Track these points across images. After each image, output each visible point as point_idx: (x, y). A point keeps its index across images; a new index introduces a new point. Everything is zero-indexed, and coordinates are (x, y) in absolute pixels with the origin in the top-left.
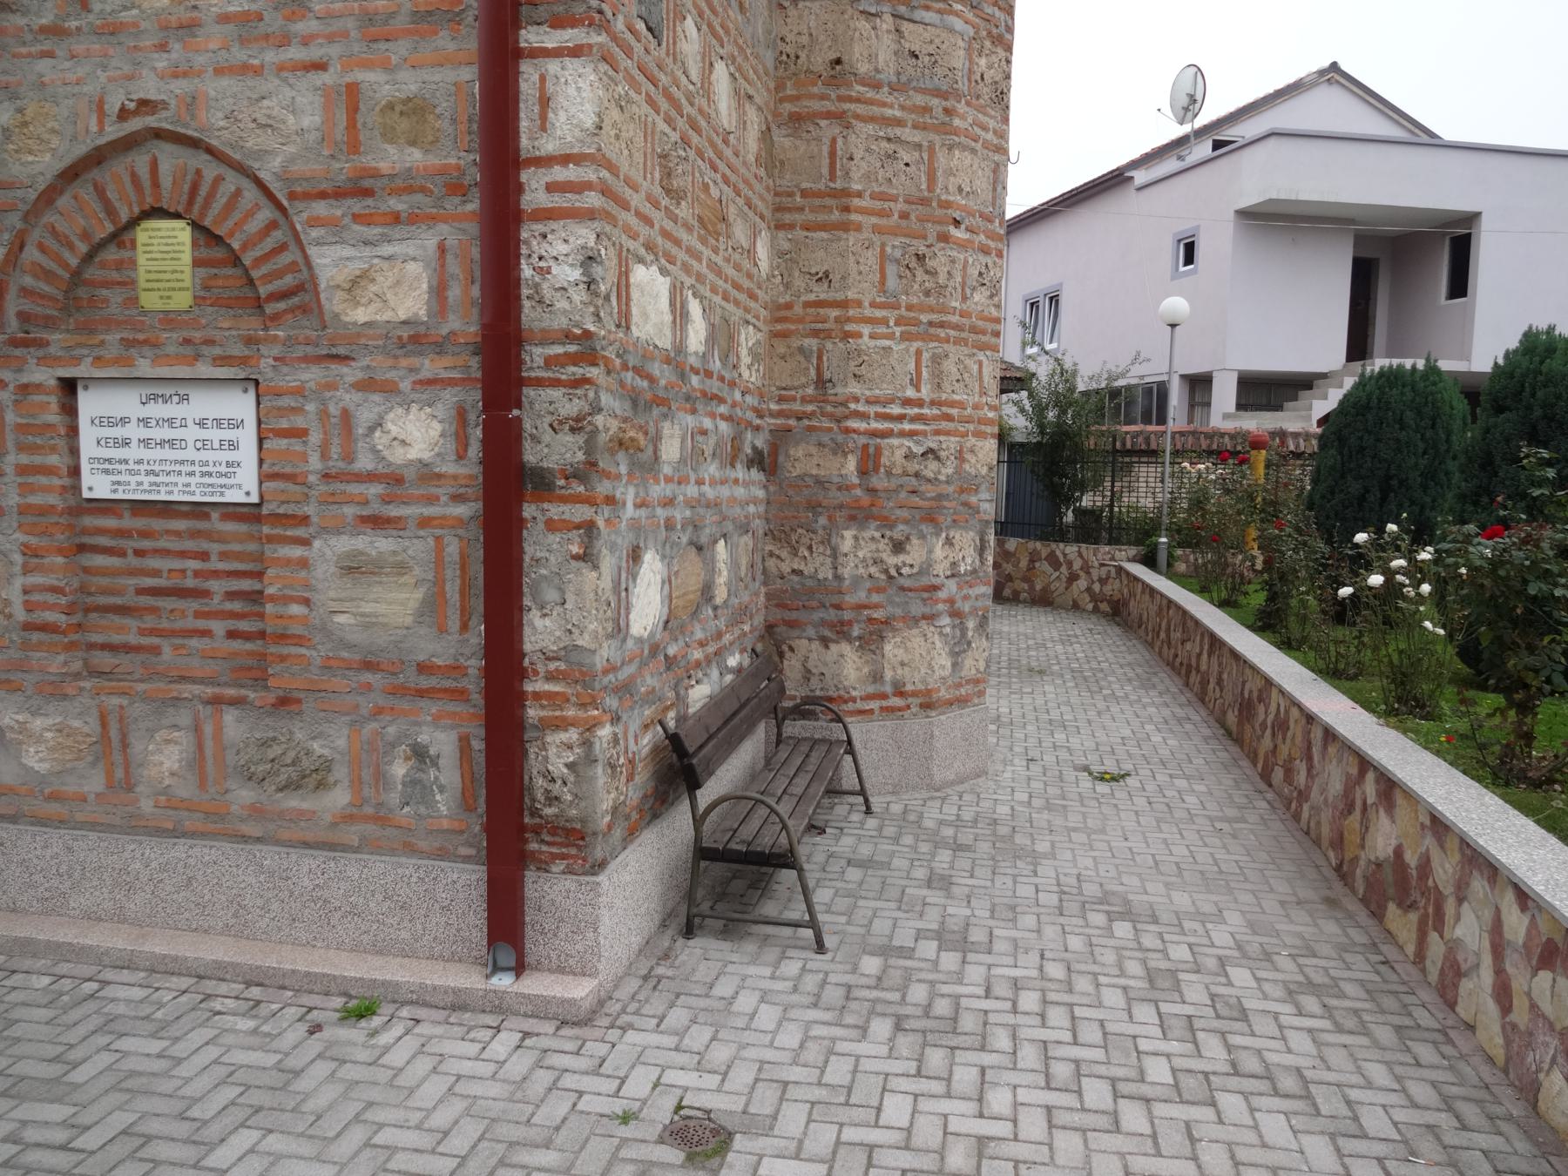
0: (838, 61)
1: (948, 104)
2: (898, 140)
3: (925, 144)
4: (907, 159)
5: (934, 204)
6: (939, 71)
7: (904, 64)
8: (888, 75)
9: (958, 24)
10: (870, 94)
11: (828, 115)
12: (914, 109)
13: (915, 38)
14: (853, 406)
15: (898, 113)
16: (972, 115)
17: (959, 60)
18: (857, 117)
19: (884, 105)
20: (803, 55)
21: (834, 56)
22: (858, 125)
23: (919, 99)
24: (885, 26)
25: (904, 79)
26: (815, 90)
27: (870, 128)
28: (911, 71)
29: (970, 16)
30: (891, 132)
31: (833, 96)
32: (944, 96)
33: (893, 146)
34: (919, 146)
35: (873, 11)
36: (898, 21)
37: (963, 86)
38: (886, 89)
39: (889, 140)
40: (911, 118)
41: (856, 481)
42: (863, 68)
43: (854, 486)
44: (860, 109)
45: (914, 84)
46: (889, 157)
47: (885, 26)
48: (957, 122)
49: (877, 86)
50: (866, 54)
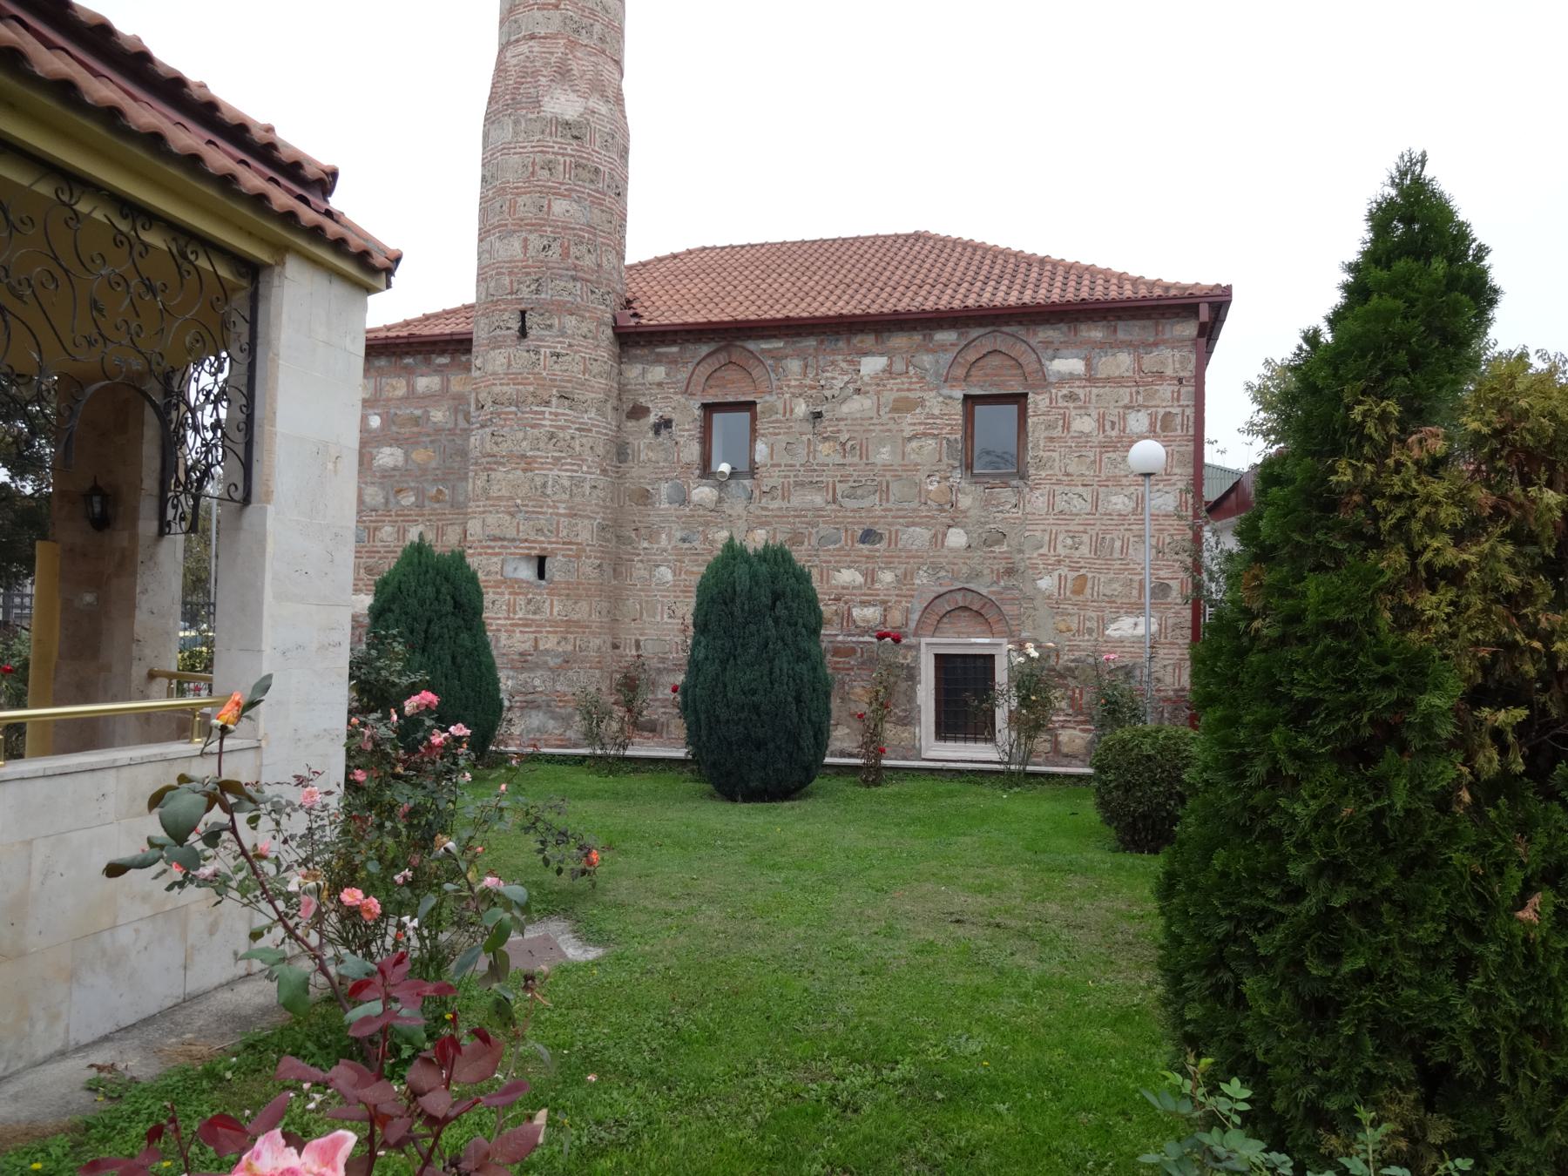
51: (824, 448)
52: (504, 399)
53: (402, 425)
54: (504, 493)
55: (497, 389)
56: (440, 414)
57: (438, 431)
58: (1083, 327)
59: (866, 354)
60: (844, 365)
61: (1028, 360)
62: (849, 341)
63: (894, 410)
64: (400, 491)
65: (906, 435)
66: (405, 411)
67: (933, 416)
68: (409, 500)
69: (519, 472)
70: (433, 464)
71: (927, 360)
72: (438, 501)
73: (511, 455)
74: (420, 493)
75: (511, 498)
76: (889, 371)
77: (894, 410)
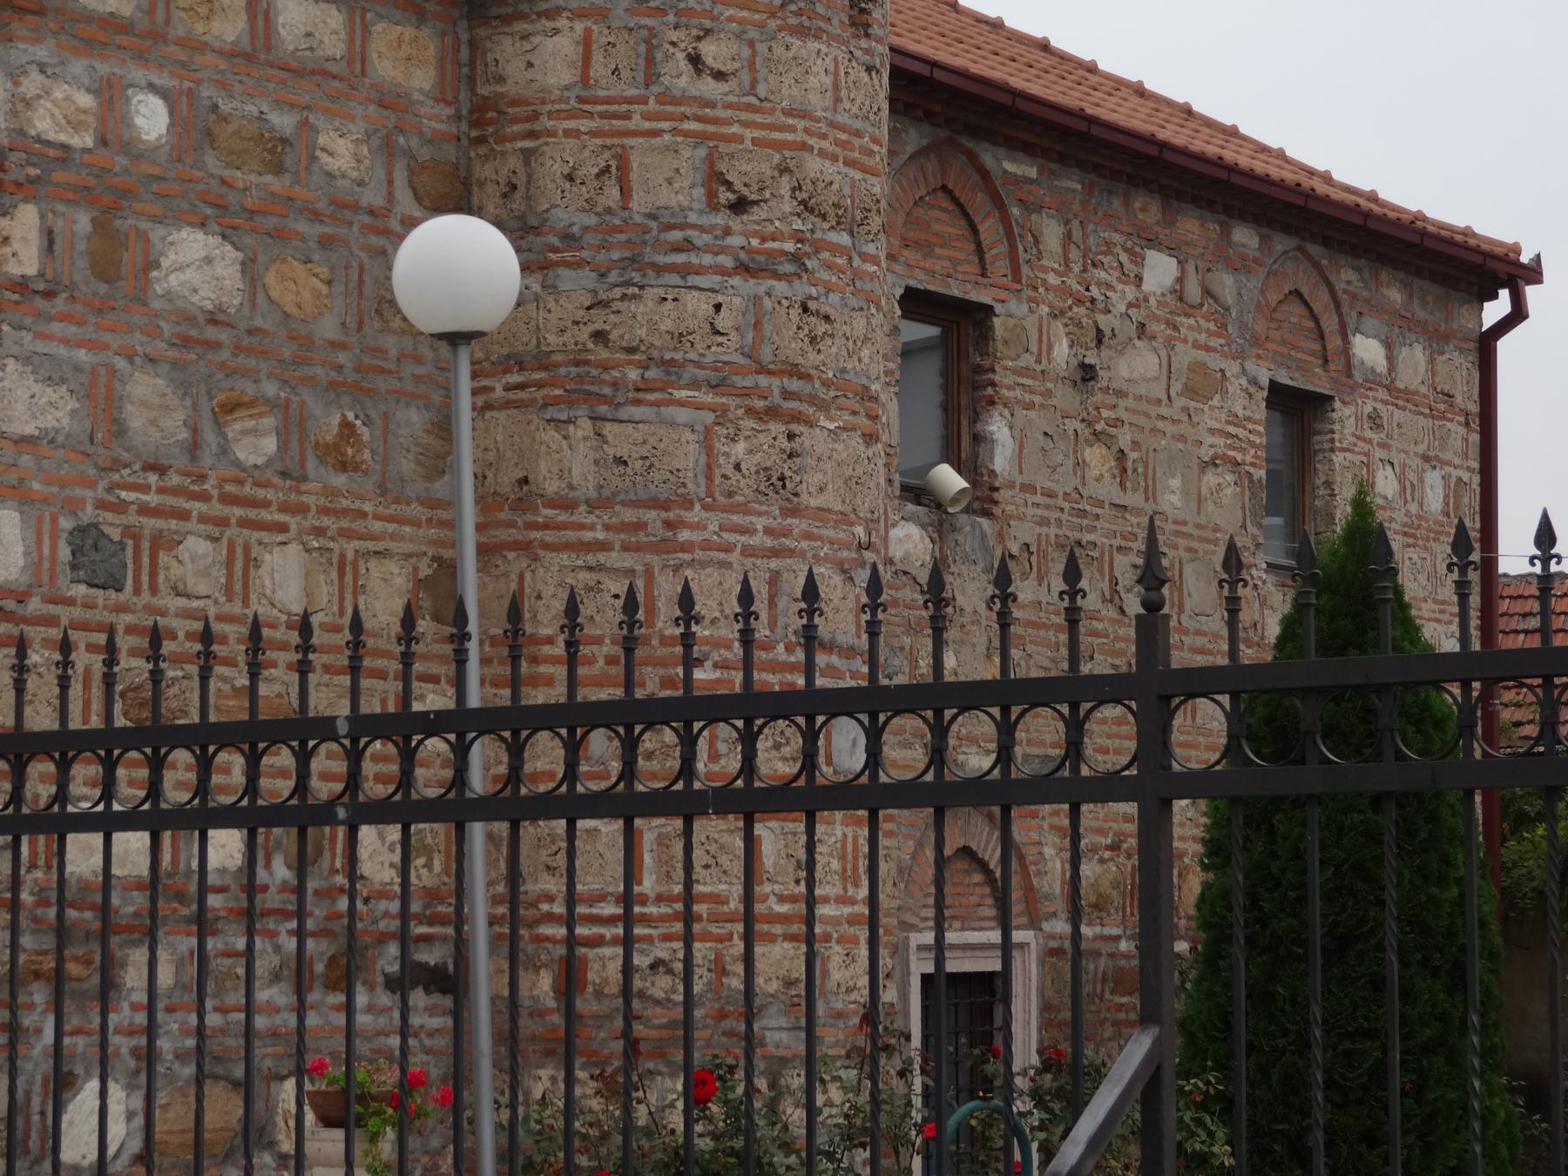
0: (525, 481)
1: (671, 515)
2: (600, 568)
3: (640, 568)
4: (614, 591)
5: (655, 642)
6: (656, 476)
7: (607, 475)
8: (588, 489)
9: (682, 415)
10: (563, 517)
11: (517, 546)
12: (623, 527)
13: (620, 439)
14: (545, 907)
15: (600, 535)
16: (714, 521)
17: (687, 456)
18: (547, 546)
19: (582, 527)
20: (490, 475)
21: (520, 474)
22: (548, 556)
23: (629, 515)
24: (580, 433)
25: (606, 493)
26: (502, 516)
27: (564, 558)
28: (617, 481)
29: (708, 398)
30: (591, 559)
31: (520, 523)
32: (665, 505)
33: (595, 576)
34: (631, 572)
35: (564, 417)
36: (599, 424)
37: (697, 488)
38: (583, 508)
39: (590, 569)
40: (617, 539)
41: (551, 1003)
42: (552, 487)
43: (549, 1011)
44: (550, 536)
45: (622, 497)
46: (591, 589)
47: (580, 433)
48: (684, 535)
49: (569, 505)
50: (555, 470)
51: (1096, 457)
52: (827, 199)
53: (236, 160)
54: (829, 500)
55: (814, 166)
56: (343, 146)
57: (344, 207)
58: (1384, 276)
59: (1152, 242)
60: (1124, 258)
61: (1330, 323)
62: (1127, 203)
63: (1189, 391)
64: (231, 407)
65: (1206, 453)
66: (244, 107)
67: (1234, 419)
68: (256, 445)
69: (856, 442)
70: (328, 328)
71: (1226, 284)
72: (343, 466)
73: (839, 382)
74: (292, 426)
75: (845, 519)
76: (1178, 292)
77: (1189, 391)
